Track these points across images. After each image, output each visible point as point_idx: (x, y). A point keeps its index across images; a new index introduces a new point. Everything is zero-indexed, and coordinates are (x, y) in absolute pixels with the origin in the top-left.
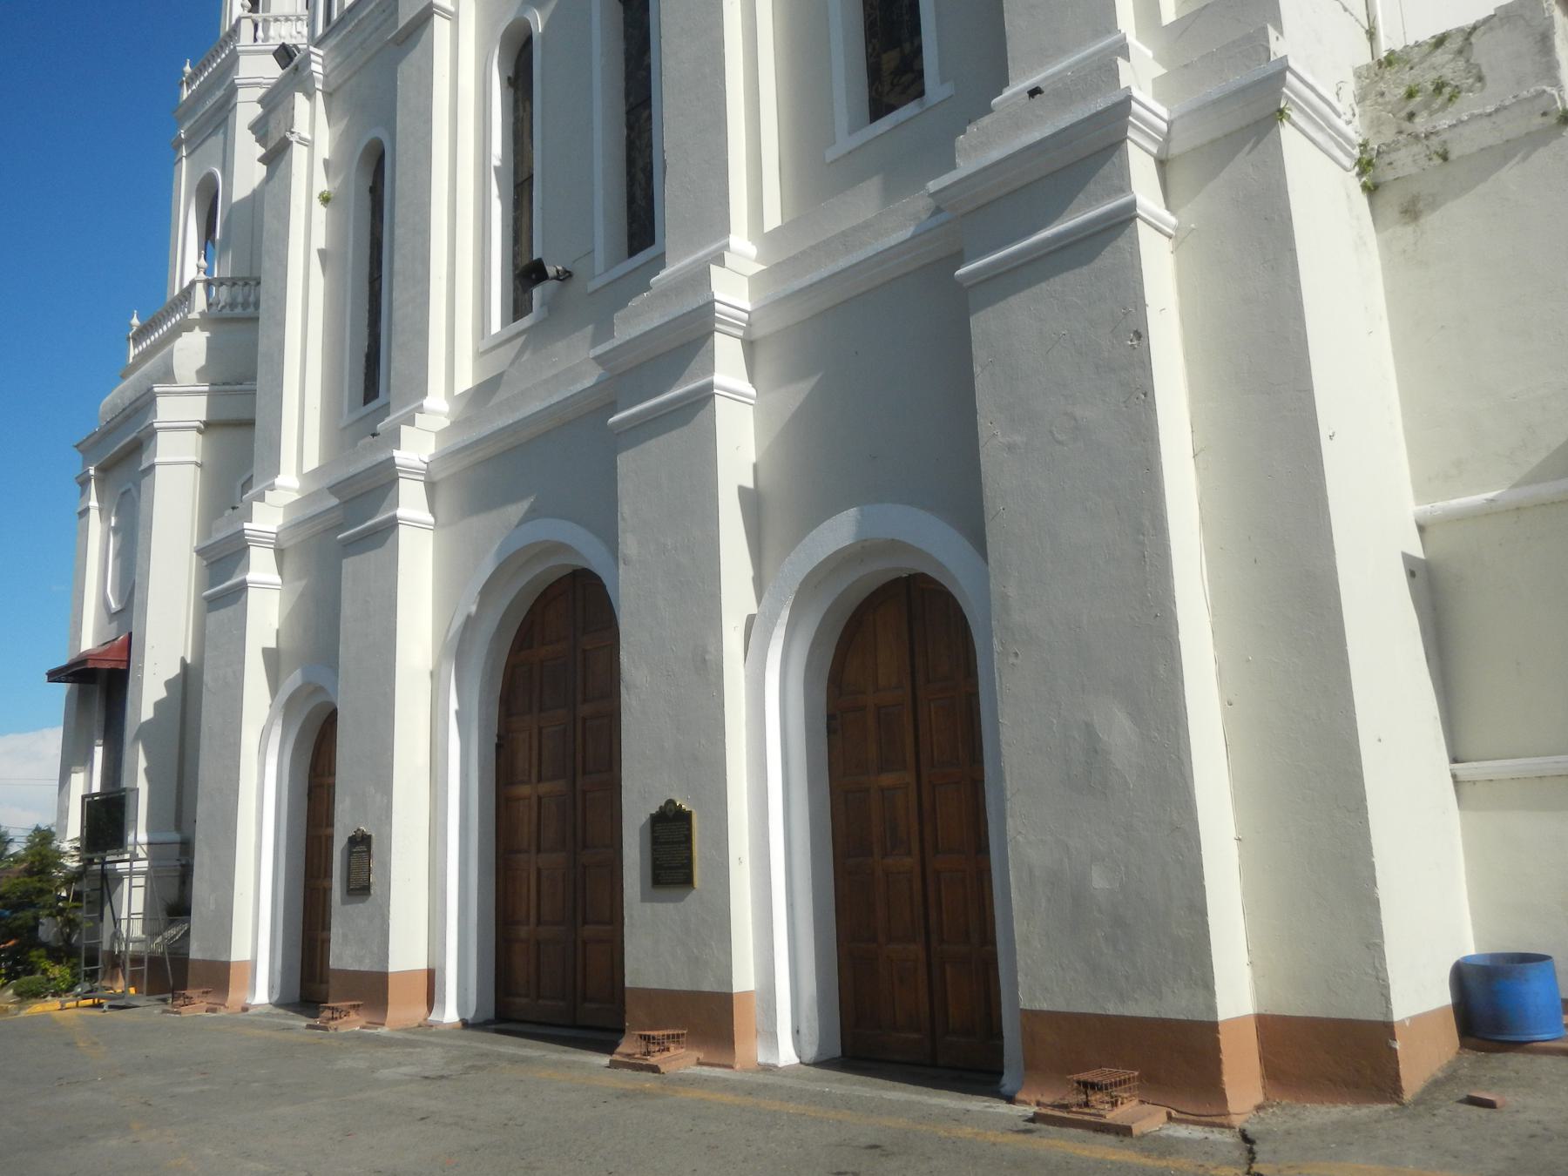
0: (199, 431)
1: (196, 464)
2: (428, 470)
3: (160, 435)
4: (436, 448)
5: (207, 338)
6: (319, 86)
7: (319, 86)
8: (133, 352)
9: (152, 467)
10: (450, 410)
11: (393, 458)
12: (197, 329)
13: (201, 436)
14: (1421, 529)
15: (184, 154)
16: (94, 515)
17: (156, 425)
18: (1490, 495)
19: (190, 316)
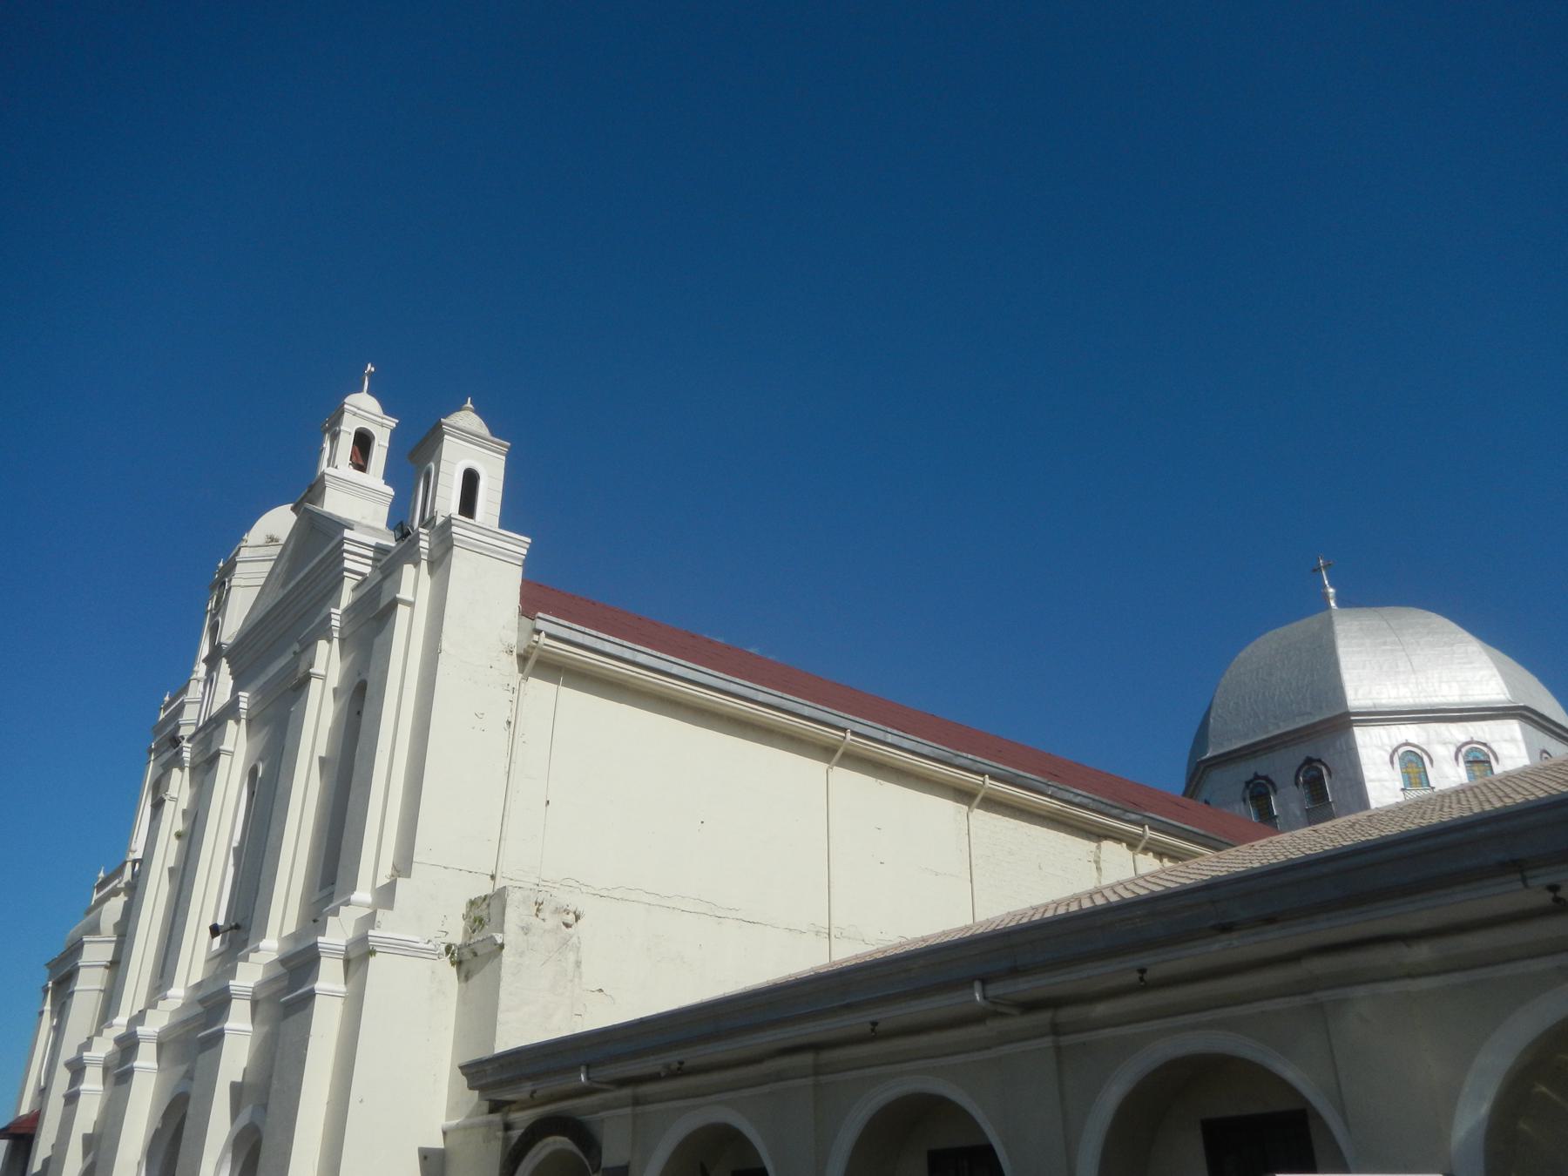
0: (106, 967)
1: (101, 990)
2: (159, 1037)
3: (82, 971)
4: (169, 1020)
5: (125, 902)
6: (187, 765)
7: (187, 765)
8: (95, 897)
9: (73, 993)
10: (279, 948)
11: (136, 1032)
12: (122, 894)
13: (107, 971)
14: (445, 1133)
15: (152, 758)
16: (47, 1015)
17: (80, 964)
18: (457, 1121)
19: (119, 886)
